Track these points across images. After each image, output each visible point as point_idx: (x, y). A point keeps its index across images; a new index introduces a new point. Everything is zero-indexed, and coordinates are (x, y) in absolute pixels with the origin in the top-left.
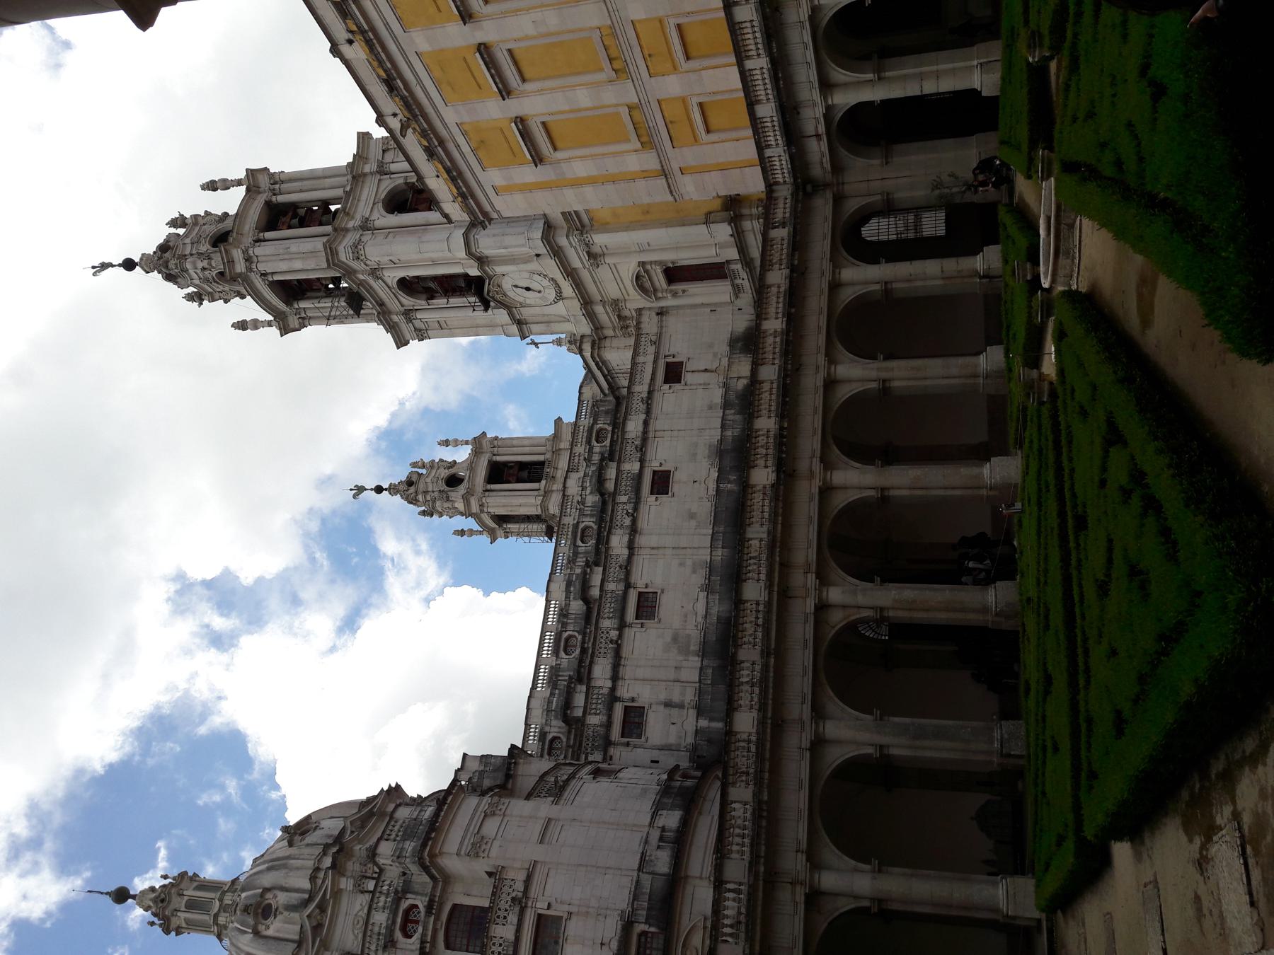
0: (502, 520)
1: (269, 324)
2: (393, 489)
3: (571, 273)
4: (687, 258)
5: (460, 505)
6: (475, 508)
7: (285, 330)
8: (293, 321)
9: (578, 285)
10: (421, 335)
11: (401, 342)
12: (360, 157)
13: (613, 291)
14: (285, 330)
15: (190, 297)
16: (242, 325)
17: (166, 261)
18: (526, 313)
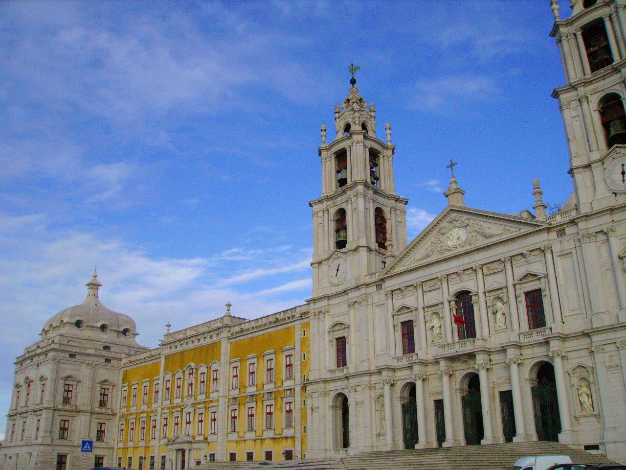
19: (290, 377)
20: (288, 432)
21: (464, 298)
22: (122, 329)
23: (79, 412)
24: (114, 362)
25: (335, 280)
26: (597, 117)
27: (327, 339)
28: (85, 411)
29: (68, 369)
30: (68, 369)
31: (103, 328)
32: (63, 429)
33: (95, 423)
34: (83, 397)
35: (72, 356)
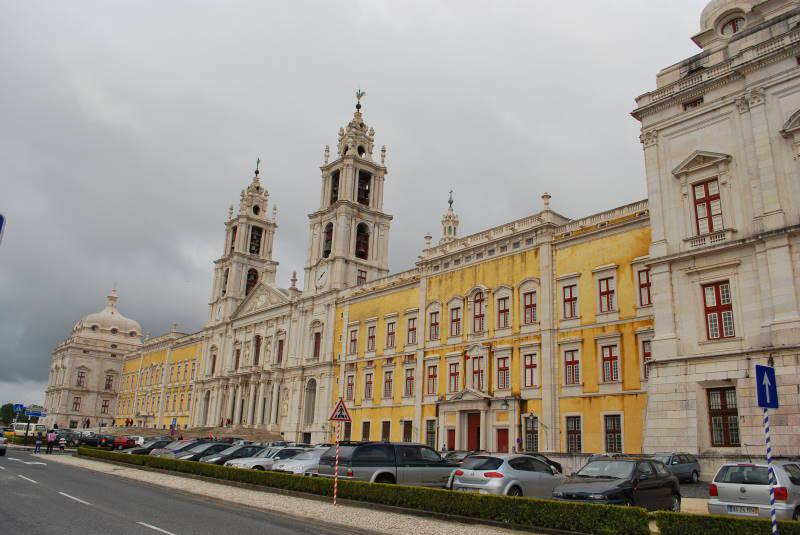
0: (235, 229)
1: (326, 162)
2: (256, 180)
3: (324, 295)
4: (323, 341)
5: (244, 213)
6: (241, 220)
7: (323, 169)
8: (326, 173)
9: (319, 297)
10: (313, 226)
11: (310, 217)
12: (382, 216)
13: (316, 310)
14: (323, 169)
15: (342, 130)
16: (327, 150)
17: (358, 126)
18: (313, 272)
19: (192, 379)
20: (187, 413)
21: (258, 339)
22: (128, 332)
23: (88, 391)
24: (118, 357)
25: (217, 318)
26: (323, 235)
27: (209, 354)
28: (93, 392)
29: (82, 361)
30: (82, 361)
31: (114, 331)
32: (105, 406)
33: (101, 400)
34: (94, 381)
35: (85, 351)
